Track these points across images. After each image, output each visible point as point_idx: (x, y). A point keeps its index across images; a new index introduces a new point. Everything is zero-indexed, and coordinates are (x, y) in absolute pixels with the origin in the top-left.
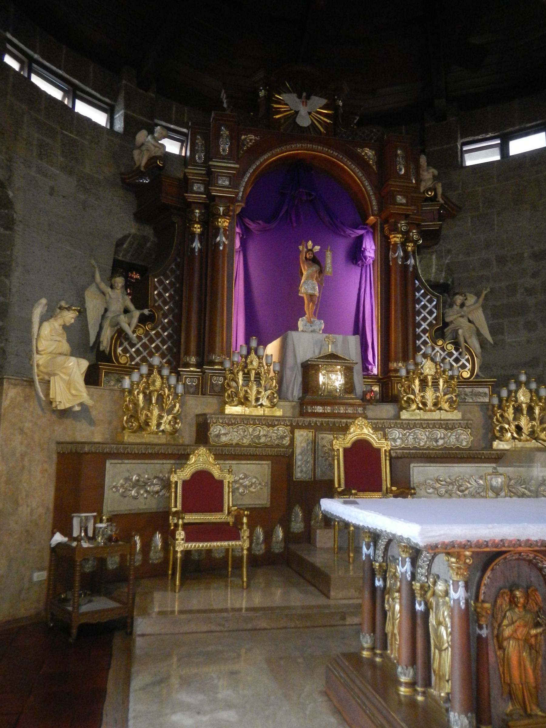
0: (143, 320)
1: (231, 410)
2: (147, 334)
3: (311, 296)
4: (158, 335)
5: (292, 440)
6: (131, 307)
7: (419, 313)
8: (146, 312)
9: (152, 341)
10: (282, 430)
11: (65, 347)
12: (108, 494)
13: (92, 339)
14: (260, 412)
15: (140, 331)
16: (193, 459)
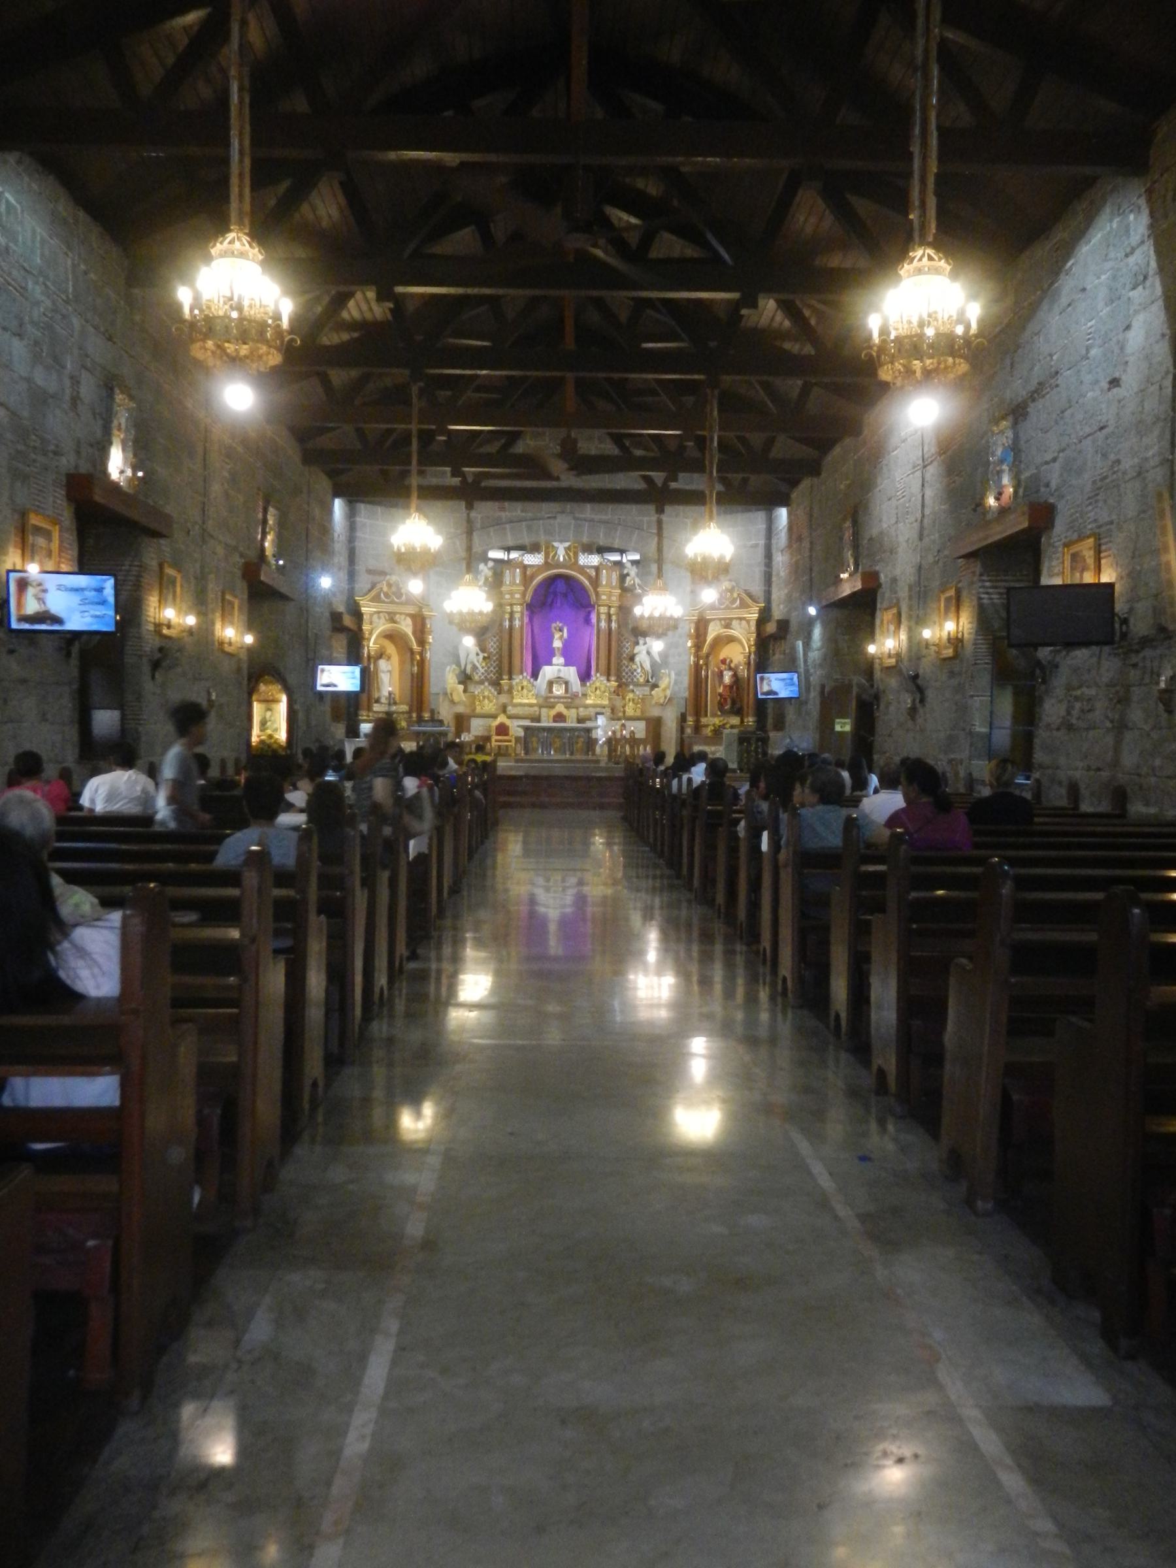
0: (484, 658)
1: (515, 701)
2: (486, 664)
3: (558, 648)
4: (491, 665)
5: (540, 712)
6: (479, 652)
7: (622, 648)
8: (486, 655)
9: (489, 668)
10: (536, 709)
11: (457, 682)
12: (472, 729)
13: (463, 667)
14: (526, 701)
15: (484, 664)
16: (499, 719)
